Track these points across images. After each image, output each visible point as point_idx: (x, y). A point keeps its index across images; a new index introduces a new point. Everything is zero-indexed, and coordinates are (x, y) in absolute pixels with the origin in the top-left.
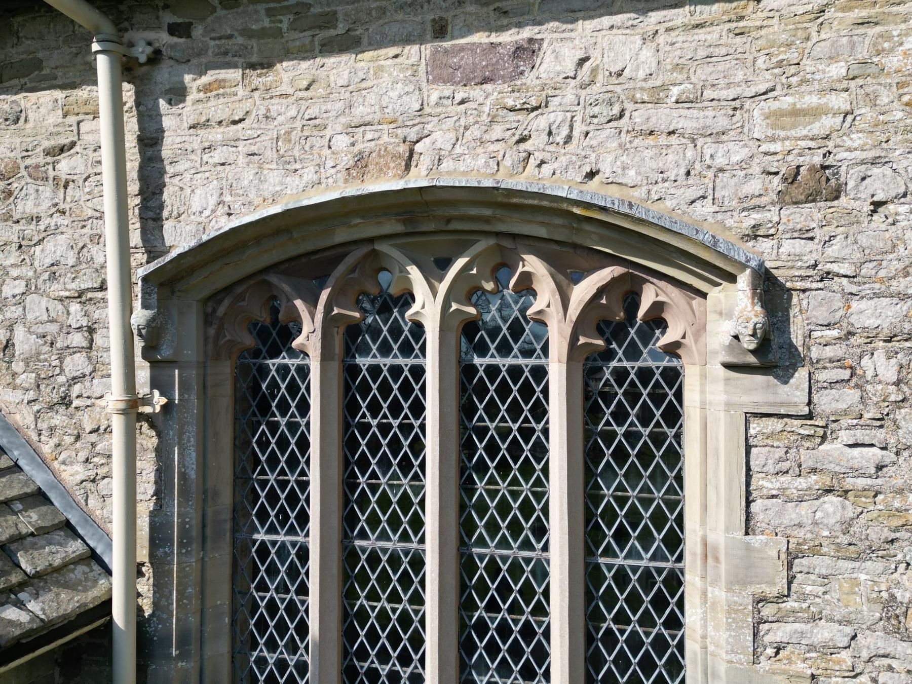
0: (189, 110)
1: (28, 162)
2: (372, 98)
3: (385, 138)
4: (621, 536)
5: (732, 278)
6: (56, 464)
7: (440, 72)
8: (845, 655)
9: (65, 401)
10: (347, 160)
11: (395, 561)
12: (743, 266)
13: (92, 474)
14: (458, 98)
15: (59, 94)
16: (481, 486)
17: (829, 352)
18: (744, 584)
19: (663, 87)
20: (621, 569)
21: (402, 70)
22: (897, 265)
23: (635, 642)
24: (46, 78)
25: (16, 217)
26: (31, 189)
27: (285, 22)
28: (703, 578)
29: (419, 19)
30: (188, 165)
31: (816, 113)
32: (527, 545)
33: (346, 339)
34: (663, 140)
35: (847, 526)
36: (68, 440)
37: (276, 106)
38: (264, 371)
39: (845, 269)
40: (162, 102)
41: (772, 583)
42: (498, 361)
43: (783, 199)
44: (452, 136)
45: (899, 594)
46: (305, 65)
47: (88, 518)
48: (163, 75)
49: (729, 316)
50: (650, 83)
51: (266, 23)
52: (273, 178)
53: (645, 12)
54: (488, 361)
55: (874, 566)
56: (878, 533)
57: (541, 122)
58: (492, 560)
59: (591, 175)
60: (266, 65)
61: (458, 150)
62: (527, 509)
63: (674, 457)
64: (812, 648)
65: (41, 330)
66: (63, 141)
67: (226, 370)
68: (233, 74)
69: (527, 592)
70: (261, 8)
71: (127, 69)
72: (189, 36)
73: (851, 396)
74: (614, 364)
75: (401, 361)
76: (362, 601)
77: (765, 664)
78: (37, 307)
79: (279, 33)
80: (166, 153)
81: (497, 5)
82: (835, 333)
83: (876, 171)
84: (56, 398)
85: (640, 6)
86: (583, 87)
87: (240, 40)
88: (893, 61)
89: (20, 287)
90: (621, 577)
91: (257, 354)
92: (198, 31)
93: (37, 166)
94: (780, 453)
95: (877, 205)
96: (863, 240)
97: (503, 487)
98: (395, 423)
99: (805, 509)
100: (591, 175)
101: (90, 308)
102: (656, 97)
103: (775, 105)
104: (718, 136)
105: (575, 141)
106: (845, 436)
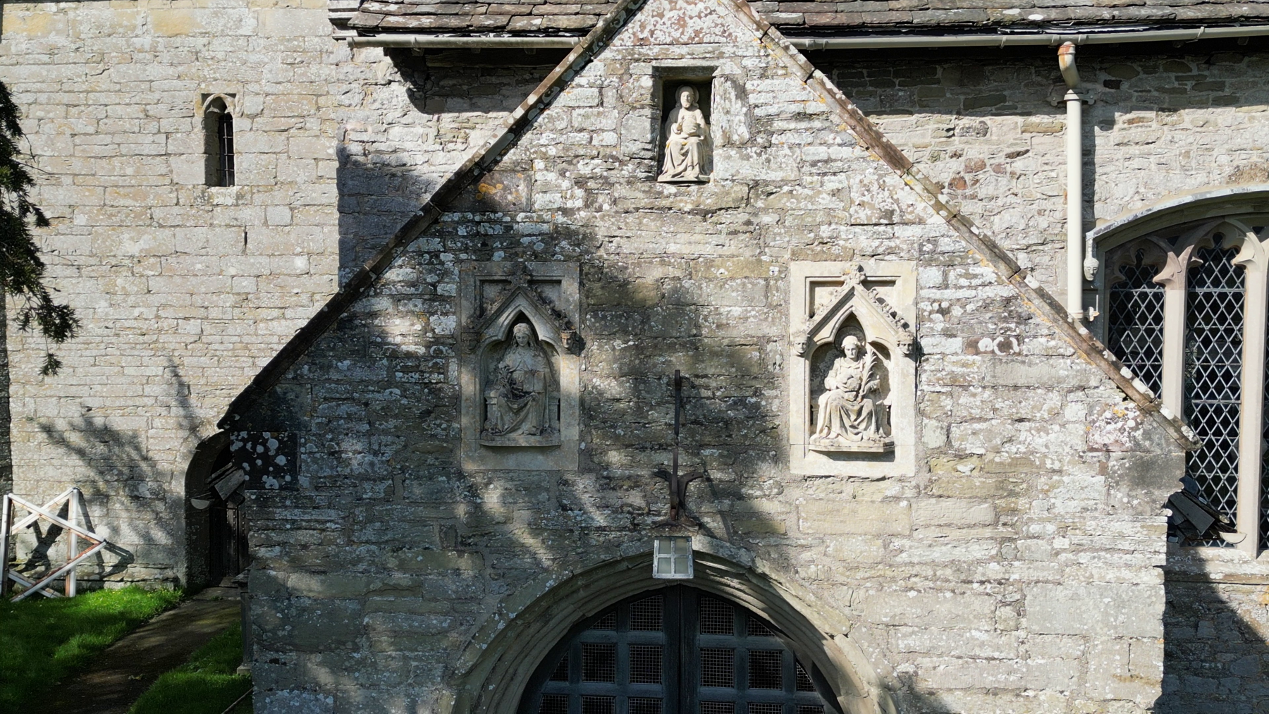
0: (1115, 134)
2: (1247, 135)
3: (1255, 159)
10: (1228, 170)
11: (1218, 411)
15: (1019, 120)
24: (1009, 108)
25: (980, 196)
27: (1189, 85)
30: (1113, 168)
33: (1194, 276)
37: (1178, 135)
38: (1131, 296)
40: (1097, 128)
48: (1099, 112)
51: (1176, 85)
52: (1176, 178)
60: (1173, 109)
68: (1151, 114)
70: (1173, 75)
72: (1118, 88)
75: (1226, 290)
80: (1098, 159)
87: (1156, 94)
91: (1124, 285)
92: (1125, 86)
98: (1222, 328)
101: (1033, 256)
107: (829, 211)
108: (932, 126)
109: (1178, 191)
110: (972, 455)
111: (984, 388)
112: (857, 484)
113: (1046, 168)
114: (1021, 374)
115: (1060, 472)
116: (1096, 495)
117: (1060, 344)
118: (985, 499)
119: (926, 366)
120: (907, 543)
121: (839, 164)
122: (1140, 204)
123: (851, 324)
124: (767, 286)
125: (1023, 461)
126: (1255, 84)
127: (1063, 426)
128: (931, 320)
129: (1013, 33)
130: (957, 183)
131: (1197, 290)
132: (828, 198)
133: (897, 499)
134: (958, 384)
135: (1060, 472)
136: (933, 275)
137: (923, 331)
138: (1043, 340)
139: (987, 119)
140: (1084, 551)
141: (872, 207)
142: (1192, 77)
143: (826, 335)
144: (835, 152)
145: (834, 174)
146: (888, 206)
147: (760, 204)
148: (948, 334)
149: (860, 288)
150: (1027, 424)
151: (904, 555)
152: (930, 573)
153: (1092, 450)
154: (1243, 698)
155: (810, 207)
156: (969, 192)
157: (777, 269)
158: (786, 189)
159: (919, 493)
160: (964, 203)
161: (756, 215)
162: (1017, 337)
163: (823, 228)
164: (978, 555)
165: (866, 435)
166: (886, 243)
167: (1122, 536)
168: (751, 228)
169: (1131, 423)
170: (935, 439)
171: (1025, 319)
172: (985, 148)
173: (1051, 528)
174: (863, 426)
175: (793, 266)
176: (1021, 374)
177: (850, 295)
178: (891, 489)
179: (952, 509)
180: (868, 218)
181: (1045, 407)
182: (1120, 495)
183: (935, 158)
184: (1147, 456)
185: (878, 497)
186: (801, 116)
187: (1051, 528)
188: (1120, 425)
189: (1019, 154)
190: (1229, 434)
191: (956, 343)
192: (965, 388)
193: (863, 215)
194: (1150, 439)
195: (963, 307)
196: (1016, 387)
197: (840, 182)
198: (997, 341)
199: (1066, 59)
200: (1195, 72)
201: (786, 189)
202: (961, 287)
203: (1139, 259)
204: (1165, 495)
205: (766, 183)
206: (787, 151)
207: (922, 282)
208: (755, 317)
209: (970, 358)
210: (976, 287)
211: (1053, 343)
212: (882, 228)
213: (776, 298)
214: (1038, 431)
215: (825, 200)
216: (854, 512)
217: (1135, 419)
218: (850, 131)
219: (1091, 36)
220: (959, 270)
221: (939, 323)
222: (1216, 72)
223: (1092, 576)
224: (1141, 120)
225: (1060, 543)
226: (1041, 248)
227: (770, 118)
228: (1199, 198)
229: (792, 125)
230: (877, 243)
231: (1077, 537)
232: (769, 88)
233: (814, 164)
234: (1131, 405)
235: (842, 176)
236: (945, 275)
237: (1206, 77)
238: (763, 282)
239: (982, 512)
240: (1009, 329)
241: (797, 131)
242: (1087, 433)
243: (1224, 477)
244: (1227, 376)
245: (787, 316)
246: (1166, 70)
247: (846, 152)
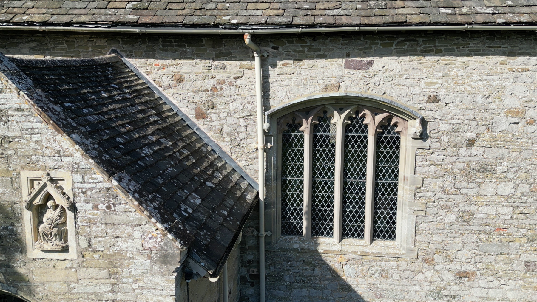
0: (277, 70)
1: (228, 80)
2: (330, 71)
3: (333, 82)
4: (384, 176)
5: (415, 119)
6: (237, 161)
7: (348, 66)
8: (433, 199)
9: (239, 145)
10: (322, 86)
11: (326, 183)
12: (418, 118)
13: (247, 164)
14: (352, 73)
15: (238, 63)
16: (349, 165)
17: (435, 135)
18: (413, 185)
19: (402, 75)
20: (383, 183)
21: (338, 65)
22: (450, 117)
23: (386, 199)
24: (234, 57)
26: (229, 88)
27: (306, 49)
28: (404, 184)
30: (277, 84)
31: (436, 83)
32: (361, 178)
33: (314, 128)
34: (401, 87)
35: (435, 172)
36: (240, 155)
37: (303, 71)
38: (290, 136)
39: (439, 118)
40: (270, 67)
41: (419, 184)
42: (355, 134)
43: (427, 102)
44: (351, 82)
45: (445, 185)
46: (311, 61)
47: (247, 175)
48: (270, 60)
49: (414, 127)
50: (400, 73)
51: (301, 49)
52: (302, 89)
53: (399, 57)
54: (352, 134)
55: (440, 180)
56: (441, 173)
57: (372, 81)
58: (352, 182)
59: (384, 94)
61: (352, 85)
62: (361, 170)
63: (397, 157)
64: (426, 197)
65: (232, 126)
66: (239, 75)
67: (280, 136)
68: (291, 62)
69: (360, 189)
70: (300, 45)
71: (263, 61)
73: (438, 145)
74: (384, 135)
76: (317, 193)
77: (416, 201)
78: (231, 120)
79: (304, 52)
80: (270, 80)
82: (436, 131)
83: (447, 97)
84: (236, 144)
85: (398, 55)
86: (384, 73)
87: (293, 53)
88: (452, 73)
89: (226, 115)
90: (383, 185)
91: (288, 131)
92: (280, 49)
93: (231, 82)
94: (422, 157)
95: (447, 104)
96: (443, 112)
97: (355, 165)
98: (327, 150)
99: (427, 169)
100: (384, 94)
102: (401, 76)
103: (427, 81)
104: (414, 87)
105: (380, 85)
106: (436, 153)
107: (35, 150)
108: (202, 65)
109: (302, 95)
110: (99, 251)
111: (102, 224)
112: (55, 262)
113: (250, 83)
114: (116, 219)
115: (133, 258)
116: (147, 268)
117: (130, 207)
118: (105, 268)
119: (79, 215)
120: (76, 285)
121: (37, 130)
122: (287, 100)
123: (49, 197)
124: (12, 180)
125: (119, 253)
126: (333, 49)
127: (133, 240)
128: (79, 196)
129: (225, 29)
130: (214, 89)
131: (317, 134)
132: (34, 144)
133: (71, 268)
134: (92, 223)
135: (133, 258)
136: (78, 177)
137: (76, 201)
138: (123, 205)
139: (225, 62)
140: (145, 289)
141: (51, 149)
142: (307, 46)
143: (37, 201)
144: (35, 125)
145: (36, 134)
146: (58, 148)
147: (6, 146)
148: (87, 202)
149: (48, 183)
150: (120, 239)
151: (75, 290)
152: (86, 297)
153: (145, 250)
154: (332, 298)
155: (27, 148)
156: (219, 93)
157: (15, 174)
158: (16, 140)
159: (79, 265)
160: (217, 98)
161: (5, 150)
162: (113, 204)
163: (33, 157)
164: (104, 290)
165: (55, 243)
166: (59, 164)
167: (158, 283)
168: (4, 156)
169: (159, 239)
170: (84, 244)
171: (116, 197)
172: (225, 75)
173: (131, 280)
174: (54, 239)
175: (22, 172)
176: (116, 219)
177: (45, 186)
178: (68, 264)
179: (92, 272)
180: (50, 153)
181: (126, 232)
182: (156, 268)
183: (204, 79)
184: (166, 253)
185: (64, 267)
186: (19, 109)
187: (131, 280)
188: (155, 240)
189: (238, 78)
190: (330, 193)
191: (89, 206)
192: (95, 224)
193: (48, 152)
194: (166, 246)
195: (91, 191)
196: (114, 224)
197: (38, 138)
198: (105, 205)
199: (247, 40)
200: (308, 44)
201: (16, 140)
202: (90, 183)
203: (294, 121)
204: (174, 268)
205: (8, 137)
206: (15, 124)
207: (74, 180)
208: (8, 193)
209: (96, 212)
210: (96, 183)
211: (127, 207)
212: (56, 158)
213: (16, 186)
214: (124, 242)
215: (32, 145)
216: (55, 273)
217: (160, 238)
218: (39, 117)
219: (255, 31)
220: (89, 176)
221: (82, 197)
222: (317, 44)
223: (148, 299)
224: (287, 64)
225: (135, 286)
226: (250, 117)
227: (7, 110)
228: (309, 98)
229: (16, 113)
230: (55, 164)
231: (141, 284)
232: (4, 97)
233: (27, 130)
234: (159, 232)
235: (39, 135)
236: (83, 177)
237: (313, 46)
238: (10, 179)
239: (104, 273)
240: (110, 201)
241: (18, 116)
242: (142, 243)
243: (328, 210)
244: (329, 169)
245: (21, 193)
246: (297, 43)
247: (39, 125)
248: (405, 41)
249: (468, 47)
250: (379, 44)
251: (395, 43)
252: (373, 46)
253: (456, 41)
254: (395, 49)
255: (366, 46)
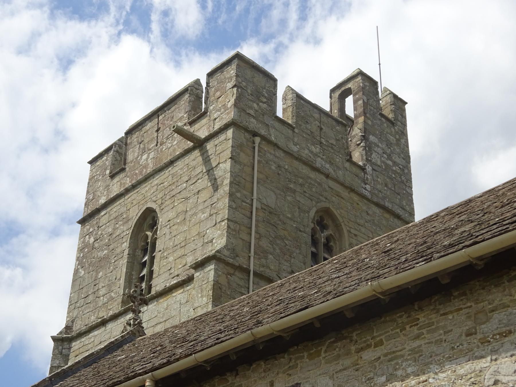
29: (266, 382)
81: (288, 372)
248: (334, 342)
249: (417, 324)
250: (306, 357)
251: (324, 348)
252: (298, 362)
253: (400, 321)
254: (324, 358)
255: (291, 364)
